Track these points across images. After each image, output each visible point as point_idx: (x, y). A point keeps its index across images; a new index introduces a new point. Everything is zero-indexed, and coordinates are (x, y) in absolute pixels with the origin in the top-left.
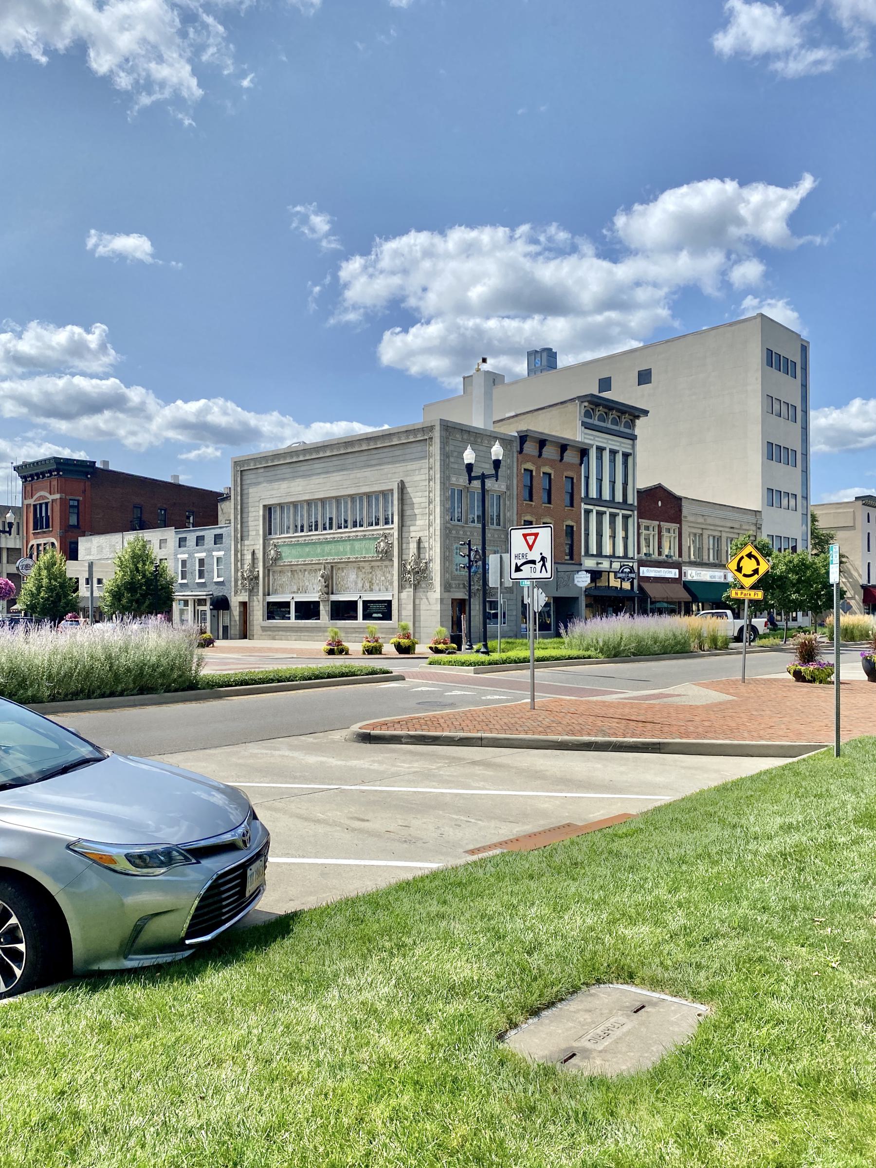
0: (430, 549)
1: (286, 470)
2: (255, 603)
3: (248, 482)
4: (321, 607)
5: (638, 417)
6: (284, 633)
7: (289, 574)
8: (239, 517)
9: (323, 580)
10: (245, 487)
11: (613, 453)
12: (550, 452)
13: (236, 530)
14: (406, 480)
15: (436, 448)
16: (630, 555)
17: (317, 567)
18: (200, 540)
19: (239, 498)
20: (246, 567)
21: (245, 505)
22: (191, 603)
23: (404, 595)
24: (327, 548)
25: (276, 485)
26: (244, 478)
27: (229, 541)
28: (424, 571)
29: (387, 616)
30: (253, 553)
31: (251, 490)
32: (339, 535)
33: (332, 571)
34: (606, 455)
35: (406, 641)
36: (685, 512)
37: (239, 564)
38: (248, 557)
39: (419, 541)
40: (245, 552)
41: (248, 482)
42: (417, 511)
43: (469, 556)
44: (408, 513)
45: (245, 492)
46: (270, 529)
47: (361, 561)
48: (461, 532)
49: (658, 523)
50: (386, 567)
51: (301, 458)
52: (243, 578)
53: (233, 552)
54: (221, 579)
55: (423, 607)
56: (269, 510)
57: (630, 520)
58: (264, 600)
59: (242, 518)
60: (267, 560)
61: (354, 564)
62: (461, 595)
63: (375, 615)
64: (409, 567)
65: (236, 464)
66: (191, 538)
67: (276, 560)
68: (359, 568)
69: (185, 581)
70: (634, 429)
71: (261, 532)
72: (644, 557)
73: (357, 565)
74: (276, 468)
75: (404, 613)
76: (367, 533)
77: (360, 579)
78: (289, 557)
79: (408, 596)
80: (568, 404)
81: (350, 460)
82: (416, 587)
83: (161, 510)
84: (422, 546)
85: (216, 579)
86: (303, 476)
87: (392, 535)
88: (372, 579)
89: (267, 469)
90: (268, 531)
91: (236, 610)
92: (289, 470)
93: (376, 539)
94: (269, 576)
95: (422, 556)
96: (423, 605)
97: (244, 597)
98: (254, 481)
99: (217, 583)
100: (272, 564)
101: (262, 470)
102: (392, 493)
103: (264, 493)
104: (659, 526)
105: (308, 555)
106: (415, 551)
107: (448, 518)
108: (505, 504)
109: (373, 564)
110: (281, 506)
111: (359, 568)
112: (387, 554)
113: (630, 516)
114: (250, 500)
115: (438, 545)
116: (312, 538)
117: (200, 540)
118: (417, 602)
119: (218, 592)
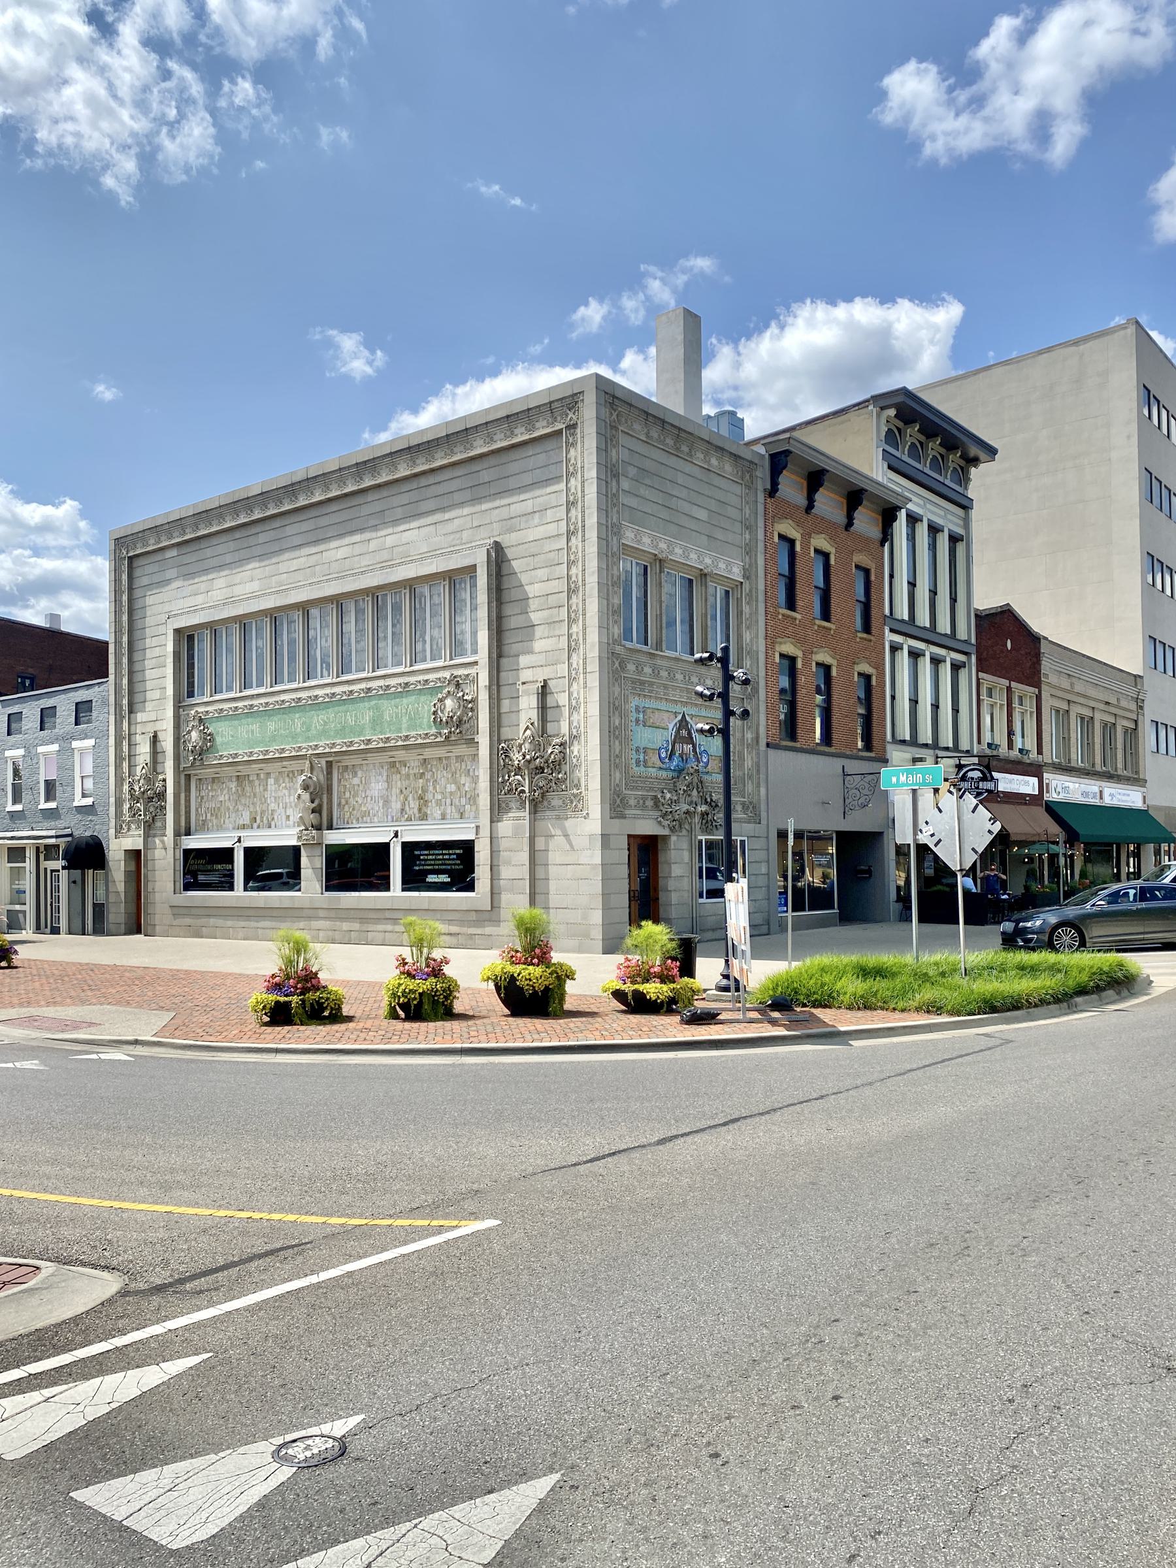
0: (573, 709)
1: (224, 547)
2: (158, 853)
3: (145, 581)
4: (304, 861)
5: (975, 461)
7: (233, 785)
8: (125, 660)
9: (306, 796)
10: (138, 593)
11: (934, 530)
12: (828, 503)
14: (506, 540)
15: (585, 453)
16: (964, 745)
17: (295, 765)
18: (46, 716)
19: (125, 618)
22: (30, 854)
23: (505, 827)
24: (318, 719)
25: (202, 582)
26: (137, 573)
27: (105, 717)
28: (557, 765)
29: (462, 879)
30: (155, 739)
31: (150, 600)
32: (346, 688)
33: (329, 773)
34: (922, 530)
35: (536, 971)
36: (1046, 666)
37: (125, 765)
38: (144, 749)
39: (544, 691)
40: (138, 738)
42: (535, 617)
43: (724, 696)
44: (513, 622)
46: (191, 684)
48: (647, 670)
49: (1006, 682)
50: (460, 759)
51: (257, 515)
54: (88, 801)
55: (554, 857)
56: (186, 639)
57: (963, 674)
59: (131, 661)
60: (183, 754)
61: (384, 758)
62: (647, 827)
63: (431, 878)
64: (516, 757)
65: (120, 542)
66: (31, 711)
67: (202, 752)
68: (393, 765)
69: (19, 807)
70: (966, 488)
71: (170, 691)
72: (988, 752)
74: (204, 543)
75: (506, 872)
76: (412, 679)
77: (395, 791)
78: (235, 740)
79: (517, 832)
80: (851, 415)
82: (536, 806)
83: (23, 678)
84: (550, 701)
86: (262, 557)
87: (475, 680)
88: (425, 791)
89: (185, 549)
90: (186, 689)
92: (232, 545)
93: (435, 690)
94: (188, 790)
95: (551, 728)
96: (556, 853)
97: (133, 840)
98: (156, 578)
99: (81, 809)
100: (196, 761)
101: (174, 552)
102: (473, 578)
103: (178, 603)
104: (1009, 689)
105: (273, 739)
106: (534, 715)
107: (616, 631)
108: (740, 613)
109: (428, 753)
110: (213, 627)
112: (459, 729)
113: (963, 665)
114: (149, 621)
115: (594, 697)
117: (46, 716)
118: (540, 843)
119: (83, 831)
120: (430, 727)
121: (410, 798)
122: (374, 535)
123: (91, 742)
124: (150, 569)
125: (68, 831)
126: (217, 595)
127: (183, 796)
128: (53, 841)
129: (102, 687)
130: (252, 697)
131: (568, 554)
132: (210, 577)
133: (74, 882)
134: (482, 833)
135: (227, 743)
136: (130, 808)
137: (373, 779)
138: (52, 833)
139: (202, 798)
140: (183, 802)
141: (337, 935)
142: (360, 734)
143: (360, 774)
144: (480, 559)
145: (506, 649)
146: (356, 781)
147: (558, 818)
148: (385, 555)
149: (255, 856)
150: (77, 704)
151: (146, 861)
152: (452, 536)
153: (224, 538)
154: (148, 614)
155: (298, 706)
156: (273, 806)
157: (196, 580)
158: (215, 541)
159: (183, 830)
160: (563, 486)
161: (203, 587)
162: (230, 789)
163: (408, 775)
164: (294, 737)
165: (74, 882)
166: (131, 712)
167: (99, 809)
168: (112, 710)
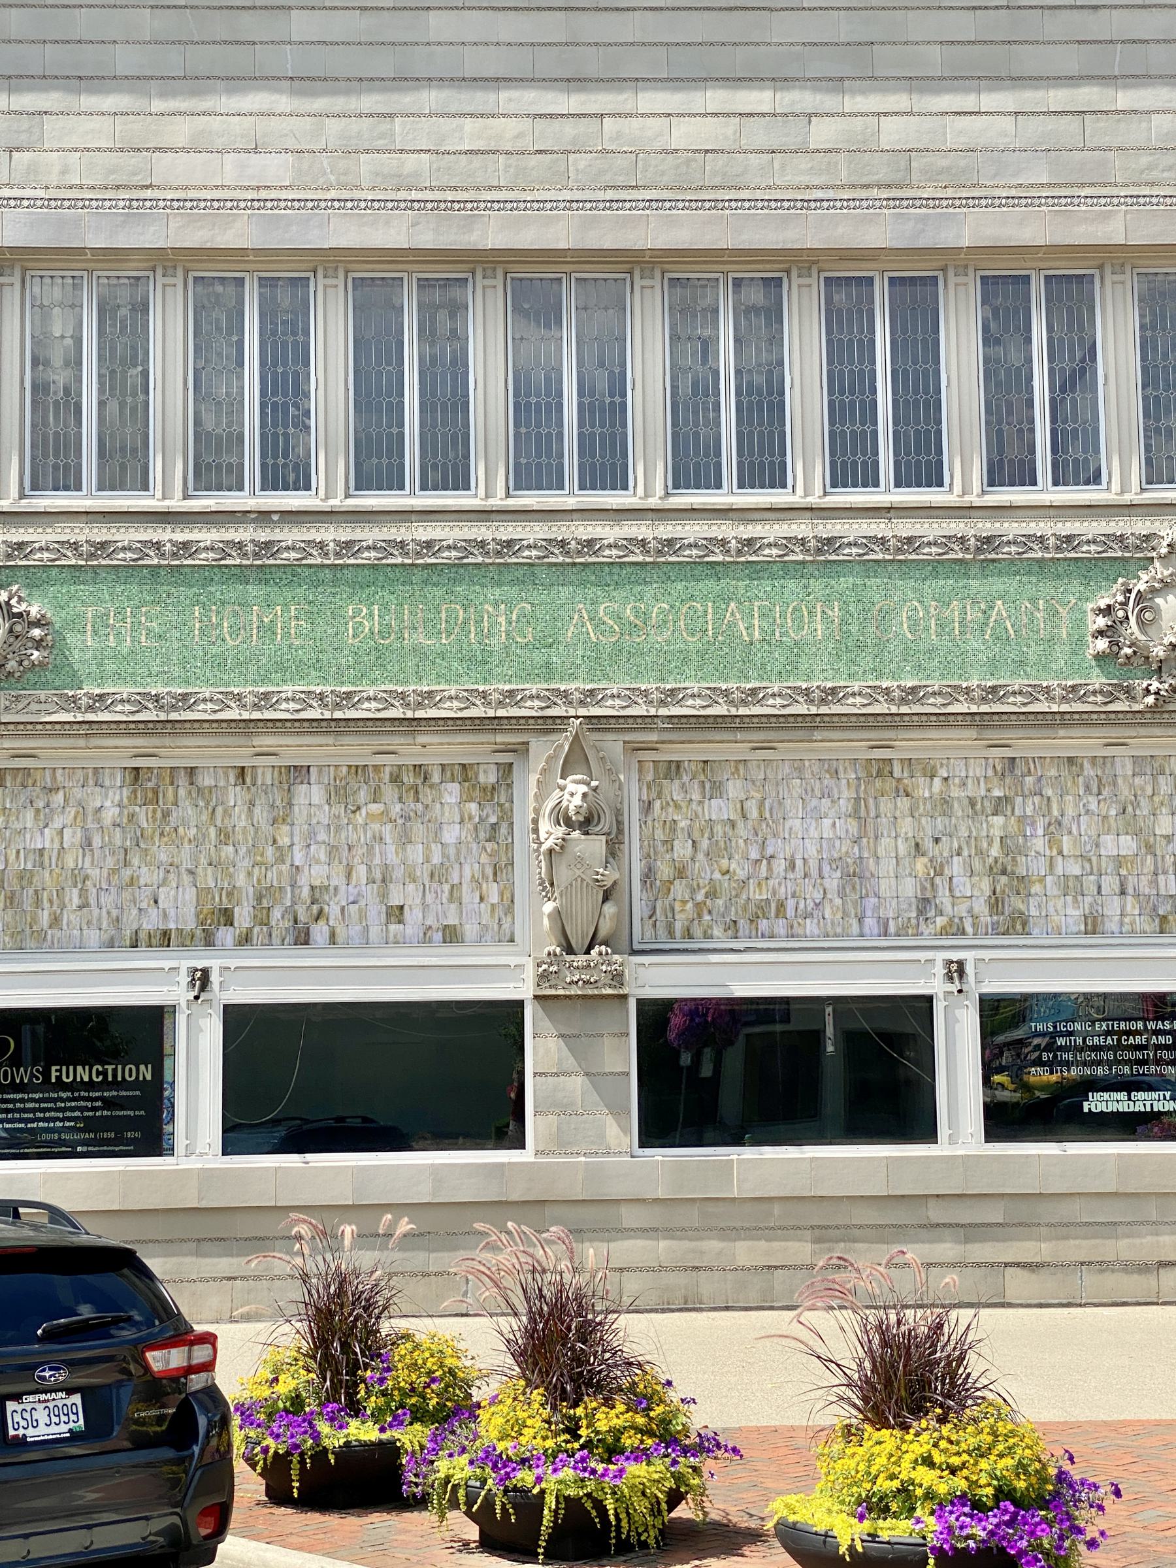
7: (110, 802)
47: (945, 720)
61: (857, 747)
73: (877, 739)
86: (303, 83)
105: (376, 659)
109: (1025, 745)
111: (883, 769)
116: (423, 532)
121: (956, 867)
122: (829, 102)
130: (264, 516)
132: (27, 101)
135: (133, 659)
137: (793, 806)
141: (707, 1286)
143: (734, 789)
146: (718, 809)
149: (254, 1036)
152: (1145, 159)
155: (497, 566)
156: (316, 874)
163: (944, 804)
164: (479, 660)
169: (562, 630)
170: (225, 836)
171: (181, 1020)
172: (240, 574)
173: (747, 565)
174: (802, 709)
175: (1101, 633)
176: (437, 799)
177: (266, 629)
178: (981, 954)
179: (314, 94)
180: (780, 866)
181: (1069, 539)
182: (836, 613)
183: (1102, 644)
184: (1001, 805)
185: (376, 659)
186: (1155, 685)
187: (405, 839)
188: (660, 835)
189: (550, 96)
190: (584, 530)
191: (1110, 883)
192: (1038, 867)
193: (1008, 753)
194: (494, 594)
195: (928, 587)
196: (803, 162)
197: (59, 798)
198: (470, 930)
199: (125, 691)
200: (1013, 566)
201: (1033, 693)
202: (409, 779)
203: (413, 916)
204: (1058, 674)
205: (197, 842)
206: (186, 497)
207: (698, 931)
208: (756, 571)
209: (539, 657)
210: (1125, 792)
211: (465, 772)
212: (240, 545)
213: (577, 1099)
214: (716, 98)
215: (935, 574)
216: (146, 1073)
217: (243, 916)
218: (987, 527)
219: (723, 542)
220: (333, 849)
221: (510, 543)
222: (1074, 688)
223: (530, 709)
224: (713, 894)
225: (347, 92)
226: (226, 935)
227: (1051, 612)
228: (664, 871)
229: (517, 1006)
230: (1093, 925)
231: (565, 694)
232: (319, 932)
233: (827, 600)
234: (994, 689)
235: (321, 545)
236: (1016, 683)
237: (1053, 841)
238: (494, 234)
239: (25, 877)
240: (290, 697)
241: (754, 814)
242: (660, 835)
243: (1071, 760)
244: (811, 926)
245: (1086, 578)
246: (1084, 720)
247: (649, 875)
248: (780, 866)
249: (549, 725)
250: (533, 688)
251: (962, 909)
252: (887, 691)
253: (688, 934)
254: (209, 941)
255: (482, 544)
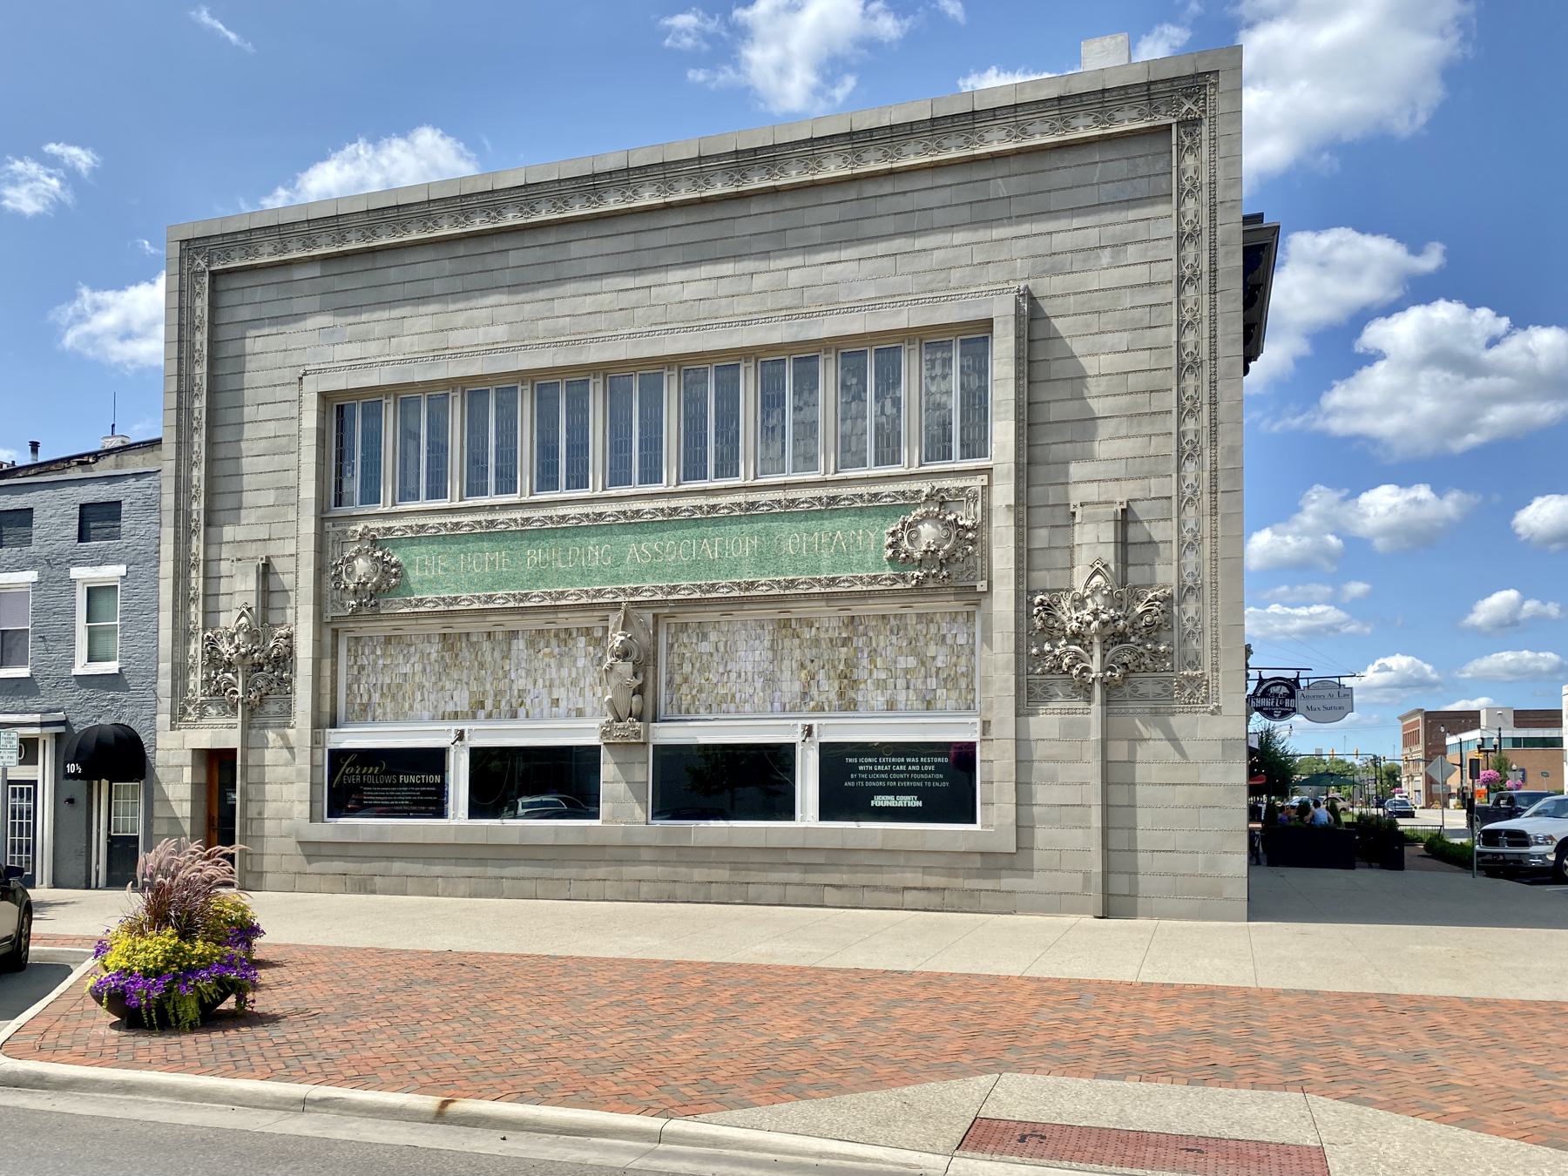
6: (416, 868)
7: (434, 650)
8: (199, 440)
10: (224, 333)
13: (182, 487)
14: (1045, 286)
20: (228, 620)
21: (224, 399)
24: (637, 549)
25: (377, 320)
26: (226, 299)
37: (196, 611)
38: (241, 587)
41: (245, 313)
42: (1098, 406)
45: (231, 350)
47: (808, 597)
52: (213, 659)
53: (167, 568)
58: (316, 742)
61: (771, 613)
64: (1071, 619)
67: (375, 596)
71: (308, 492)
73: (780, 610)
74: (381, 261)
78: (434, 578)
79: (1072, 733)
81: (759, 219)
84: (1134, 533)
85: (82, 667)
86: (514, 288)
88: (851, 664)
89: (335, 268)
91: (177, 786)
92: (448, 266)
94: (335, 655)
97: (222, 733)
101: (315, 271)
105: (539, 576)
106: (1109, 554)
109: (859, 609)
111: (786, 624)
116: (561, 511)
119: (91, 716)
120: (880, 567)
121: (821, 675)
122: (761, 265)
123: (121, 570)
124: (259, 294)
125: (60, 716)
126: (410, 344)
127: (327, 663)
128: (36, 731)
129: (144, 482)
130: (492, 508)
131: (1179, 311)
133: (71, 801)
134: (994, 731)
135: (435, 583)
136: (208, 681)
137: (741, 645)
138: (37, 718)
139: (362, 668)
140: (327, 672)
141: (679, 890)
142: (733, 571)
143: (713, 637)
144: (1002, 311)
145: (1038, 451)
146: (705, 647)
147: (1156, 712)
148: (787, 299)
150: (82, 506)
151: (245, 767)
153: (430, 254)
154: (249, 366)
155: (596, 527)
156: (521, 683)
157: (473, 303)
158: (408, 258)
159: (327, 719)
160: (1170, 209)
161: (378, 329)
162: (424, 656)
163: (816, 642)
164: (585, 574)
165: (71, 801)
166: (208, 524)
167: (133, 682)
168: (169, 518)
169: (624, 558)
170: (482, 665)
171: (452, 754)
172: (480, 537)
173: (711, 519)
174: (735, 594)
175: (890, 546)
176: (575, 645)
177: (492, 563)
178: (824, 722)
179: (519, 293)
180: (733, 676)
181: (876, 495)
182: (755, 542)
183: (890, 552)
184: (846, 642)
185: (539, 576)
186: (917, 573)
187: (560, 665)
188: (676, 661)
189: (626, 279)
190: (636, 505)
191: (901, 683)
192: (864, 675)
193: (850, 613)
194: (593, 541)
195: (802, 526)
196: (748, 299)
197: (412, 649)
198: (588, 710)
199: (431, 596)
200: (846, 511)
201: (852, 582)
202: (562, 635)
203: (563, 704)
204: (868, 569)
205: (469, 669)
206: (461, 500)
207: (692, 710)
208: (717, 522)
209: (614, 572)
210: (912, 633)
211: (588, 631)
212: (480, 523)
213: (622, 796)
214: (706, 270)
215: (806, 519)
216: (438, 779)
217: (489, 704)
218: (833, 491)
219: (701, 508)
220: (528, 672)
221: (600, 514)
222: (875, 577)
223: (608, 598)
224: (700, 691)
225: (533, 290)
226: (481, 714)
227: (866, 536)
228: (678, 679)
229: (596, 750)
230: (891, 706)
231: (624, 590)
232: (522, 712)
233: (752, 535)
234: (834, 579)
235: (515, 520)
236: (845, 576)
237: (872, 661)
238: (593, 355)
239: (399, 686)
240: (502, 597)
241: (722, 649)
242: (676, 661)
243: (884, 616)
244: (747, 707)
245: (885, 516)
246: (880, 594)
247: (670, 682)
248: (733, 676)
249: (616, 606)
250: (609, 588)
251: (823, 697)
252: (779, 582)
253: (688, 712)
254: (474, 717)
255: (587, 516)
